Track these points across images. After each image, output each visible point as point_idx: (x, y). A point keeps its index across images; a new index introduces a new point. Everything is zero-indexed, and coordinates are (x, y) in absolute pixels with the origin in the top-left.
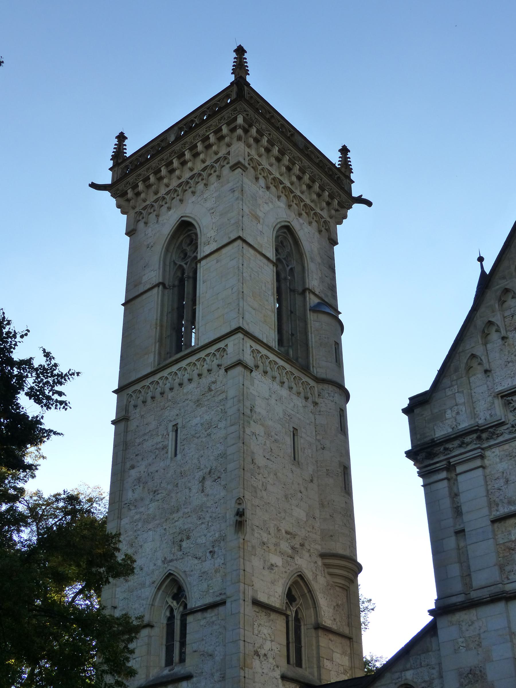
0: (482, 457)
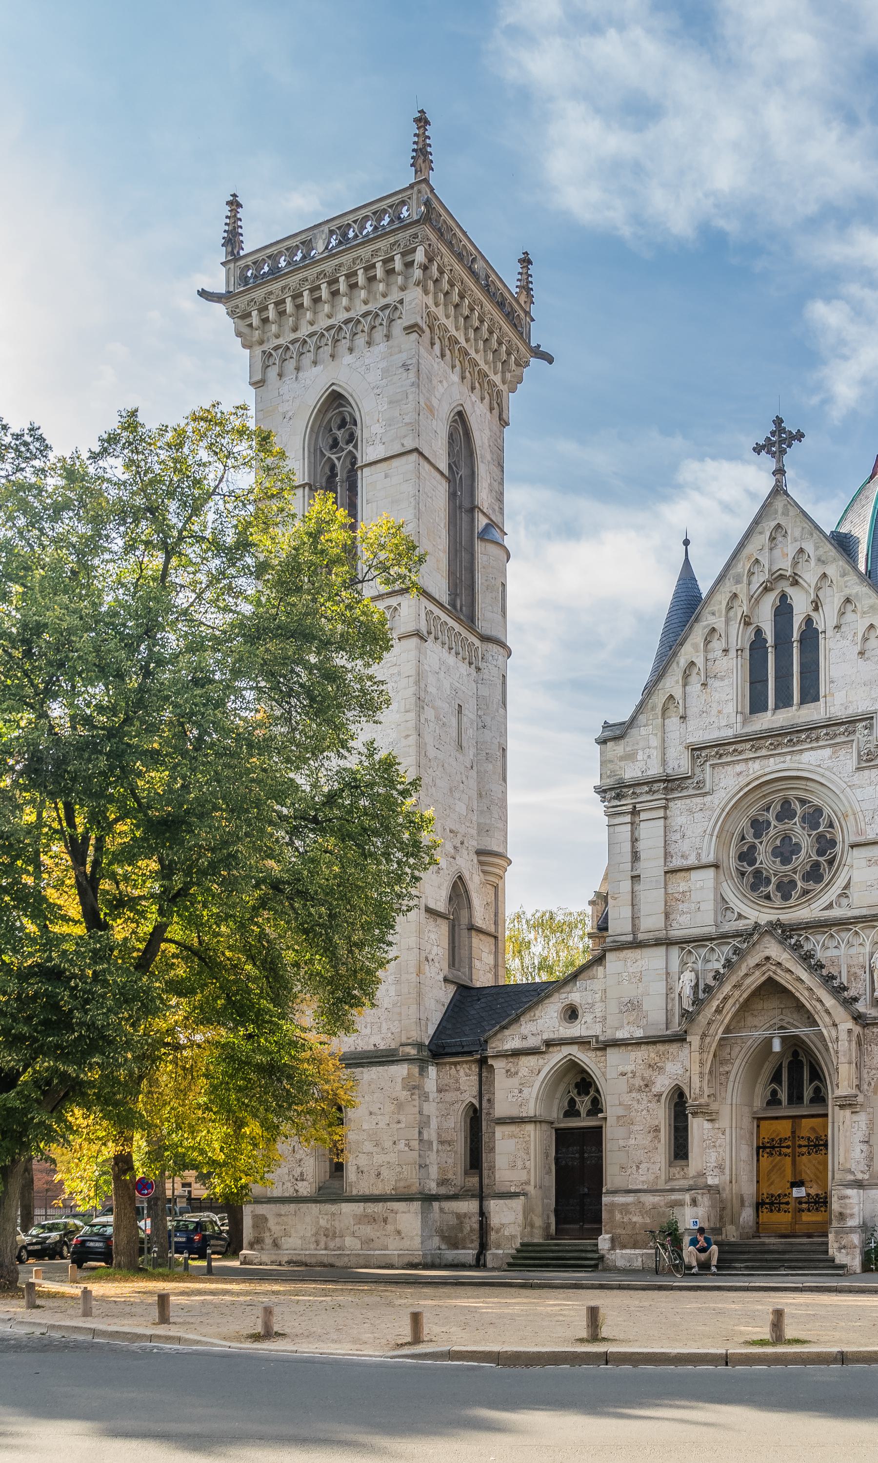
0: (666, 808)
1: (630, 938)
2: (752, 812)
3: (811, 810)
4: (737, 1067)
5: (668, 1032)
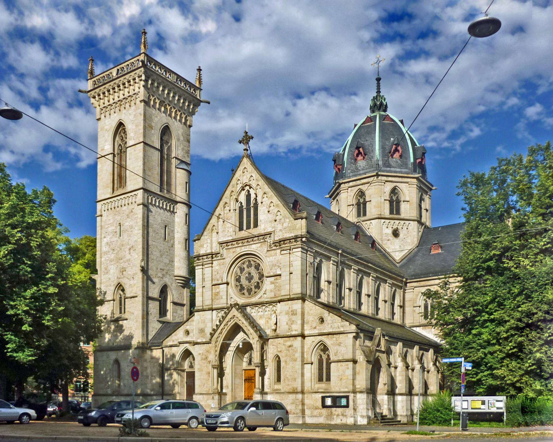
0: (212, 264)
1: (201, 308)
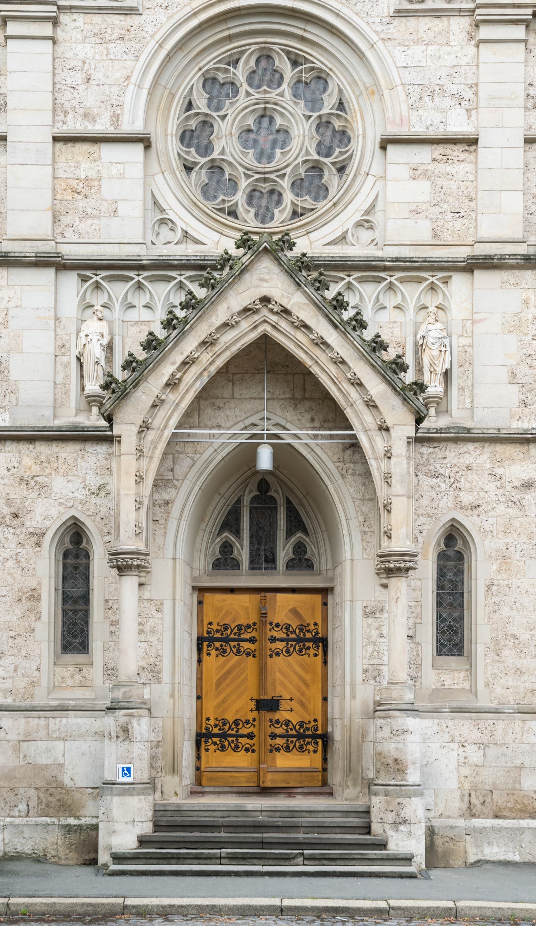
0: (55, 22)
2: (208, 61)
3: (309, 76)
4: (185, 496)
5: (58, 423)
